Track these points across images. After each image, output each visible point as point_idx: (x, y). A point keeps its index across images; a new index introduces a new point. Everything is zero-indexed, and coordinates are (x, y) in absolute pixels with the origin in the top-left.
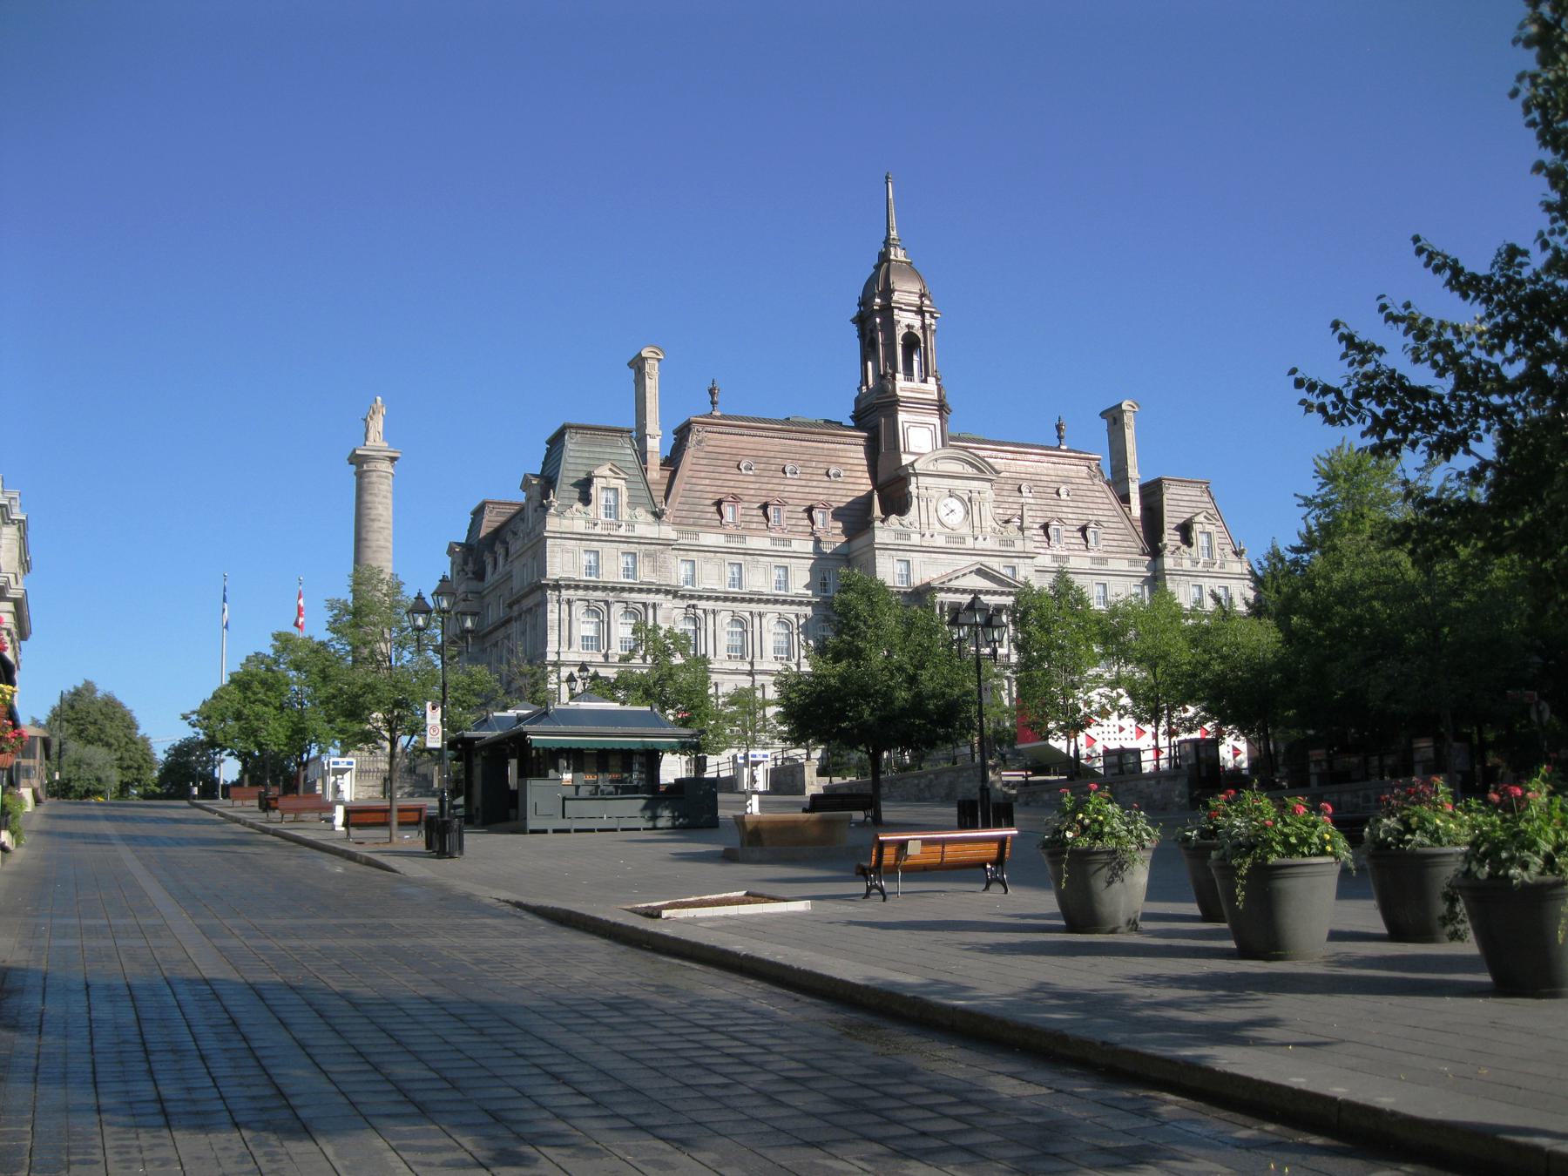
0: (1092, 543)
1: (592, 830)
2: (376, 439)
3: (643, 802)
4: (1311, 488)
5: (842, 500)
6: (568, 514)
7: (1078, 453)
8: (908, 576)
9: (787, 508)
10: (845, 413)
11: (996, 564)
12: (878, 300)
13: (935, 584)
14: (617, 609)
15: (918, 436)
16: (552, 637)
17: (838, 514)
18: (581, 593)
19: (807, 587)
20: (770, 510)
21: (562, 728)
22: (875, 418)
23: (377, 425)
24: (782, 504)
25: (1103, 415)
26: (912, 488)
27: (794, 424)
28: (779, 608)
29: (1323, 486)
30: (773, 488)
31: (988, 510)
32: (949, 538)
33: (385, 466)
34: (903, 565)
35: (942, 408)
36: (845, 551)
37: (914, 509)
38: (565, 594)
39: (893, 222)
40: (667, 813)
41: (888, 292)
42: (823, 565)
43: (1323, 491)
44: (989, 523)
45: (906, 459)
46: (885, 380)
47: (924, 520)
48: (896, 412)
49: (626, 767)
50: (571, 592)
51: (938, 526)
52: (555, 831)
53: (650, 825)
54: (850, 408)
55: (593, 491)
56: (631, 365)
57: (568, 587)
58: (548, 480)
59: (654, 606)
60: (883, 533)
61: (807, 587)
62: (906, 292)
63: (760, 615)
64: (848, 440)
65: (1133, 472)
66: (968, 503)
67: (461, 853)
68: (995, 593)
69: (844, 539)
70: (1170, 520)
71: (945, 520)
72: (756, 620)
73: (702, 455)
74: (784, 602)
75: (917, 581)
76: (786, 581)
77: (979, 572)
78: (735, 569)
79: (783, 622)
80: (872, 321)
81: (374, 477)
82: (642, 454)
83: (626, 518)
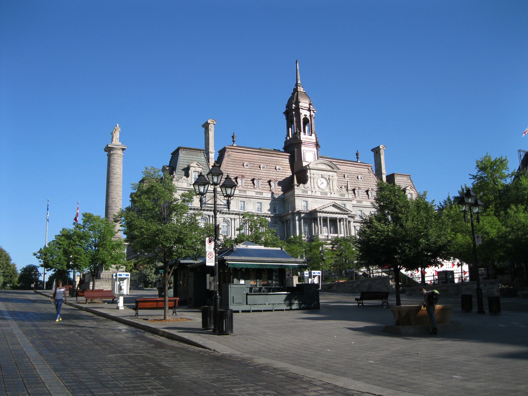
1: (260, 311)
2: (116, 142)
3: (285, 296)
4: (475, 171)
5: (281, 179)
6: (181, 180)
7: (364, 164)
8: (307, 207)
9: (261, 181)
10: (281, 146)
11: (338, 202)
12: (294, 105)
13: (318, 210)
15: (308, 155)
17: (280, 184)
19: (269, 210)
20: (255, 181)
21: (243, 258)
22: (293, 148)
23: (117, 135)
25: (372, 150)
26: (308, 174)
27: (263, 150)
29: (479, 171)
30: (256, 173)
31: (335, 183)
32: (321, 193)
33: (120, 152)
34: (305, 203)
35: (317, 145)
36: (283, 197)
37: (309, 182)
39: (299, 78)
40: (296, 302)
41: (297, 103)
42: (275, 202)
43: (479, 174)
44: (336, 188)
45: (304, 164)
46: (296, 135)
47: (312, 186)
48: (301, 146)
49: (271, 278)
51: (317, 188)
52: (243, 311)
53: (289, 308)
54: (283, 145)
55: (190, 172)
56: (203, 126)
58: (172, 168)
60: (298, 190)
61: (269, 210)
62: (304, 103)
64: (283, 156)
65: (384, 171)
67: (232, 332)
68: (339, 213)
69: (282, 193)
71: (320, 186)
73: (230, 160)
75: (310, 209)
76: (261, 208)
77: (334, 206)
78: (242, 203)
80: (291, 113)
81: (115, 156)
82: (208, 159)
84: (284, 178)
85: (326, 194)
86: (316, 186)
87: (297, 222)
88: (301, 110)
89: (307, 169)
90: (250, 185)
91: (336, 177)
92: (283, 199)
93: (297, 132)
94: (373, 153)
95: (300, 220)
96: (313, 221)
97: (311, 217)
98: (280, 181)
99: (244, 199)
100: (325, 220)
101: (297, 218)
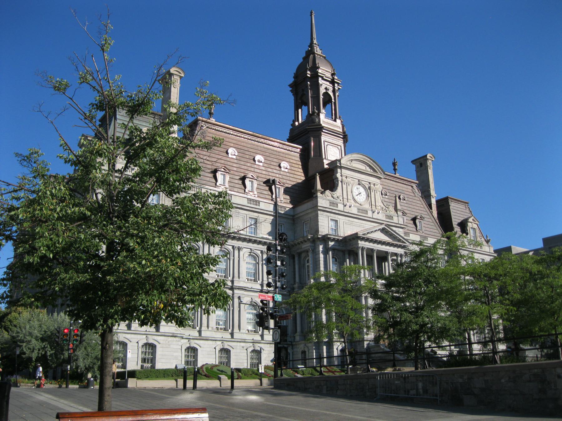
0: (418, 228)
5: (289, 184)
12: (309, 72)
13: (360, 234)
15: (332, 151)
17: (287, 191)
19: (269, 234)
22: (306, 136)
25: (412, 162)
26: (338, 175)
28: (251, 245)
35: (345, 138)
36: (292, 213)
37: (339, 188)
39: (315, 36)
41: (315, 68)
44: (379, 203)
46: (312, 118)
47: (345, 196)
48: (321, 135)
51: (352, 201)
61: (269, 234)
62: (324, 70)
63: (239, 249)
64: (290, 148)
65: (433, 193)
66: (368, 190)
69: (291, 206)
70: (456, 220)
71: (356, 198)
72: (236, 252)
74: (255, 242)
77: (383, 231)
79: (252, 255)
80: (303, 86)
84: (295, 183)
85: (366, 212)
86: (350, 197)
87: (322, 256)
88: (320, 79)
89: (337, 167)
90: (237, 186)
91: (379, 187)
92: (293, 216)
93: (313, 112)
94: (413, 167)
95: (326, 253)
96: (347, 256)
97: (347, 248)
98: (287, 187)
100: (370, 253)
101: (321, 248)
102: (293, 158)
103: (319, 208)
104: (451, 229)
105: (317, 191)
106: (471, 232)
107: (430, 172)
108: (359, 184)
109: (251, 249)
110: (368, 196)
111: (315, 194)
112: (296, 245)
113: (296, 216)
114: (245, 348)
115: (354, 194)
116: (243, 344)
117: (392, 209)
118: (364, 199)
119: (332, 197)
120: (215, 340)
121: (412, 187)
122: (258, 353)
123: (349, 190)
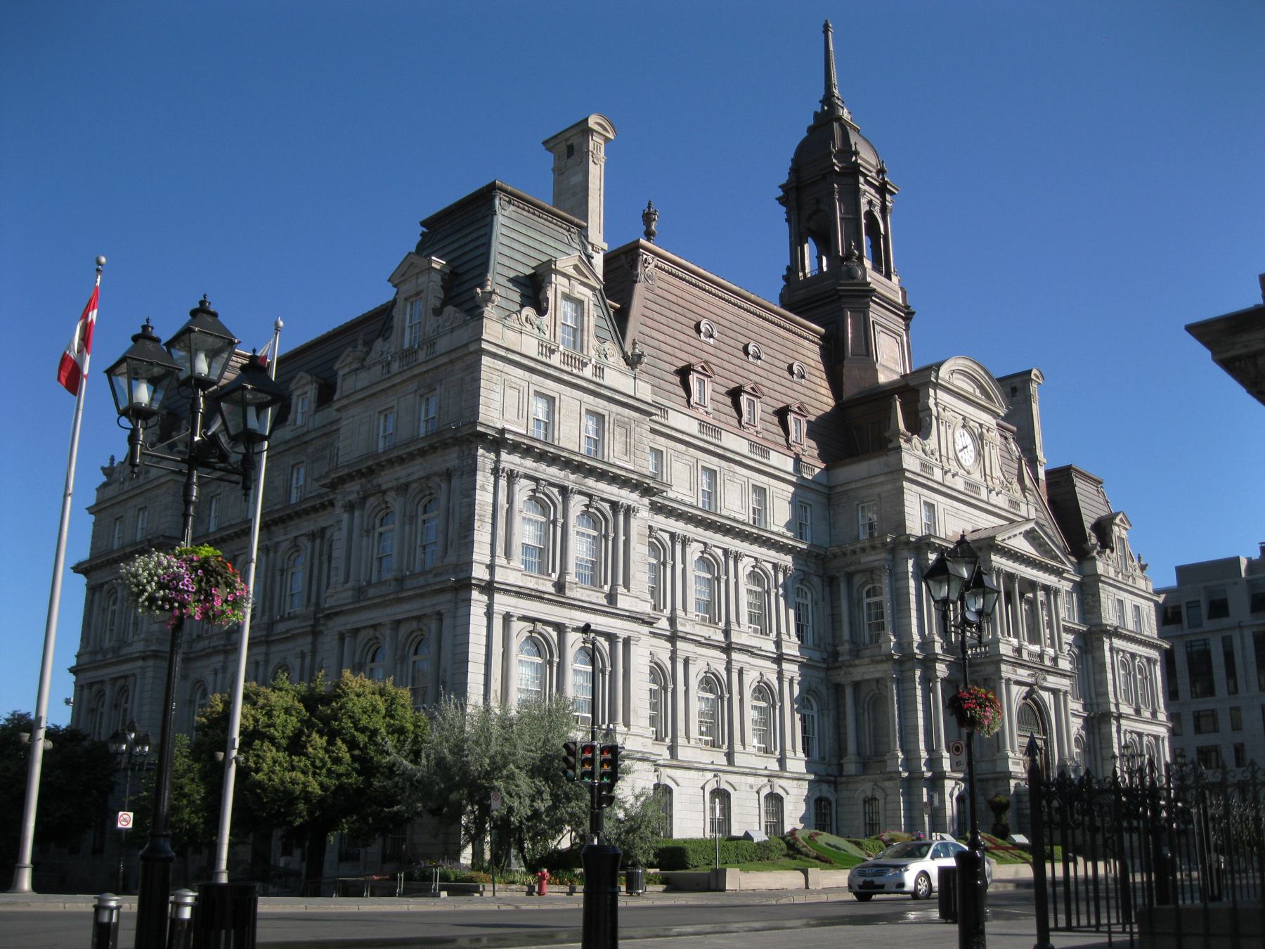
6: (513, 321)
14: (577, 504)
16: (482, 536)
18: (529, 463)
19: (789, 526)
24: (755, 393)
26: (931, 402)
35: (908, 316)
38: (510, 460)
39: (835, 80)
41: (848, 152)
42: (814, 500)
44: (997, 473)
46: (844, 266)
47: (944, 452)
50: (515, 458)
57: (515, 448)
59: (629, 511)
66: (979, 439)
71: (960, 455)
83: (592, 353)
86: (951, 455)
99: (714, 463)
102: (809, 354)
103: (907, 474)
104: (1084, 538)
105: (898, 433)
106: (1116, 544)
107: (1034, 406)
108: (964, 426)
109: (756, 559)
110: (980, 455)
111: (891, 441)
112: (845, 554)
113: (839, 489)
114: (755, 789)
115: (958, 448)
116: (751, 780)
117: (1016, 486)
118: (972, 461)
119: (924, 451)
120: (703, 770)
121: (1006, 438)
122: (775, 801)
123: (950, 437)
